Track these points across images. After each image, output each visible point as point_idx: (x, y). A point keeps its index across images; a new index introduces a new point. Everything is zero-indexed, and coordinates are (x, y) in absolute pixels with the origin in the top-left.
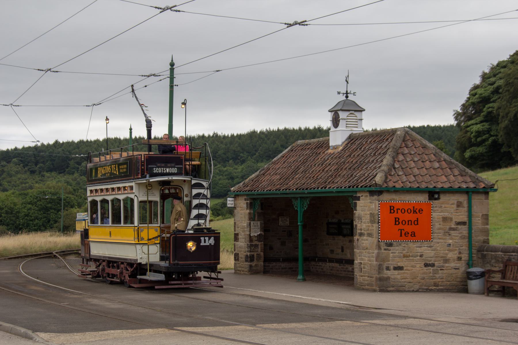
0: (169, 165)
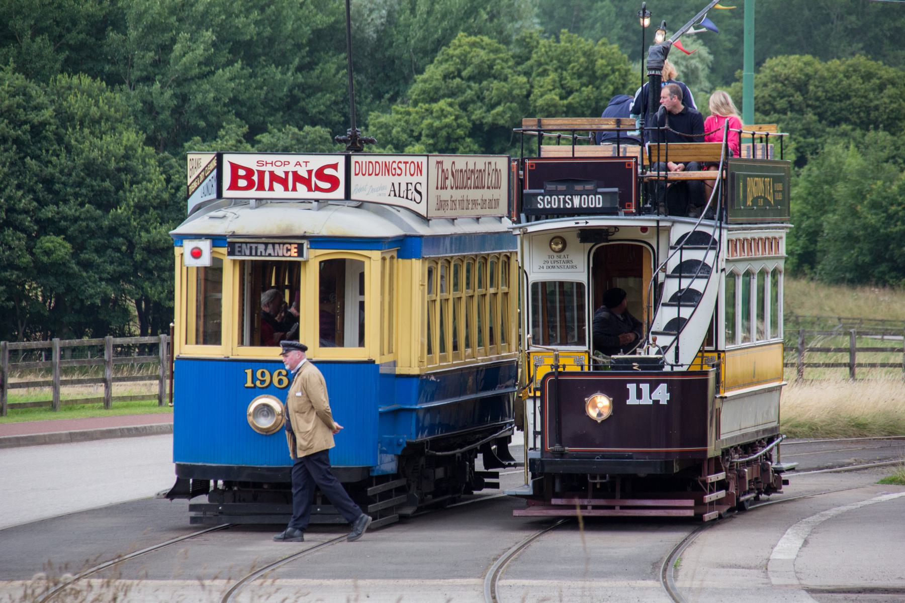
0: (578, 187)
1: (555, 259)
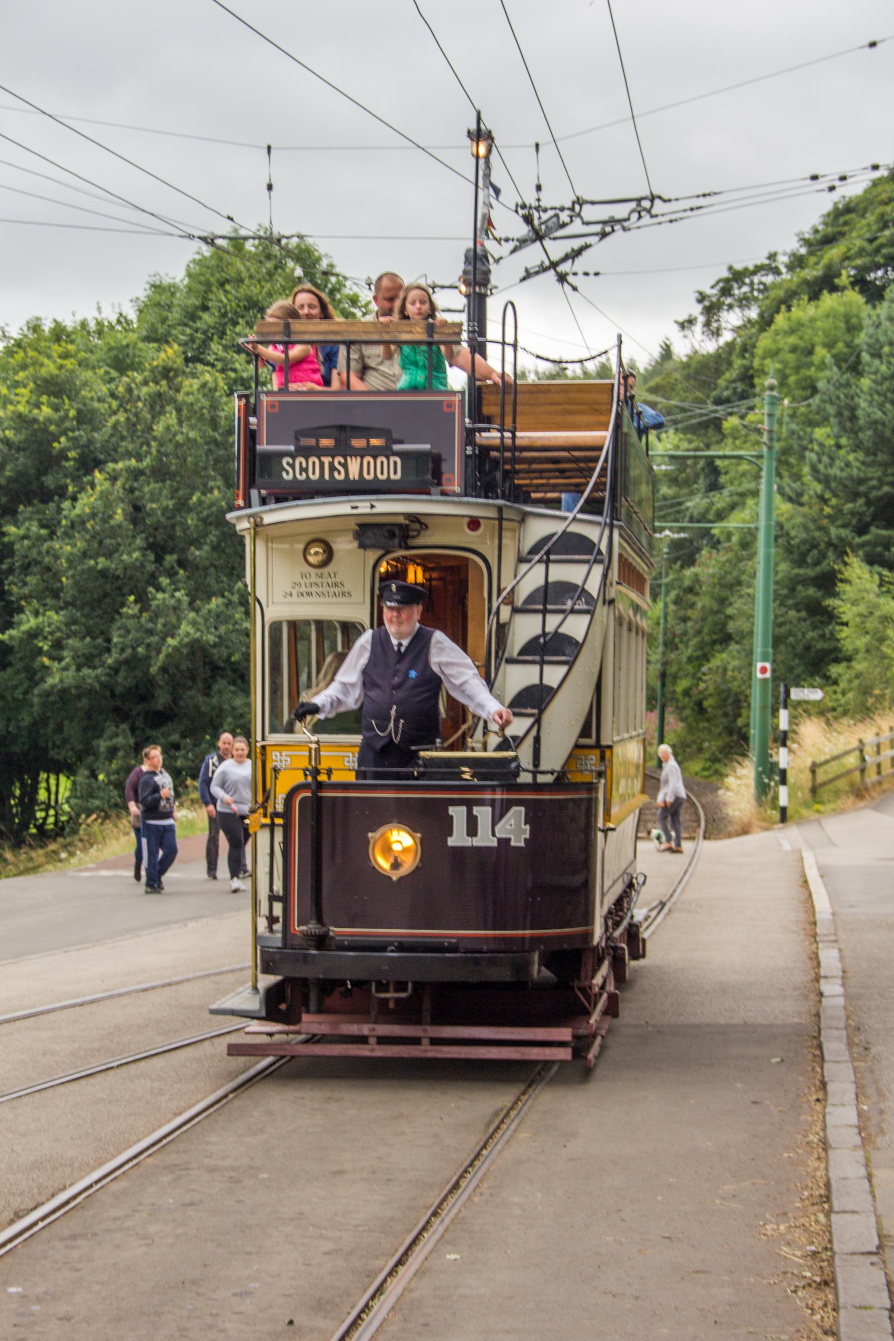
1: (314, 579)
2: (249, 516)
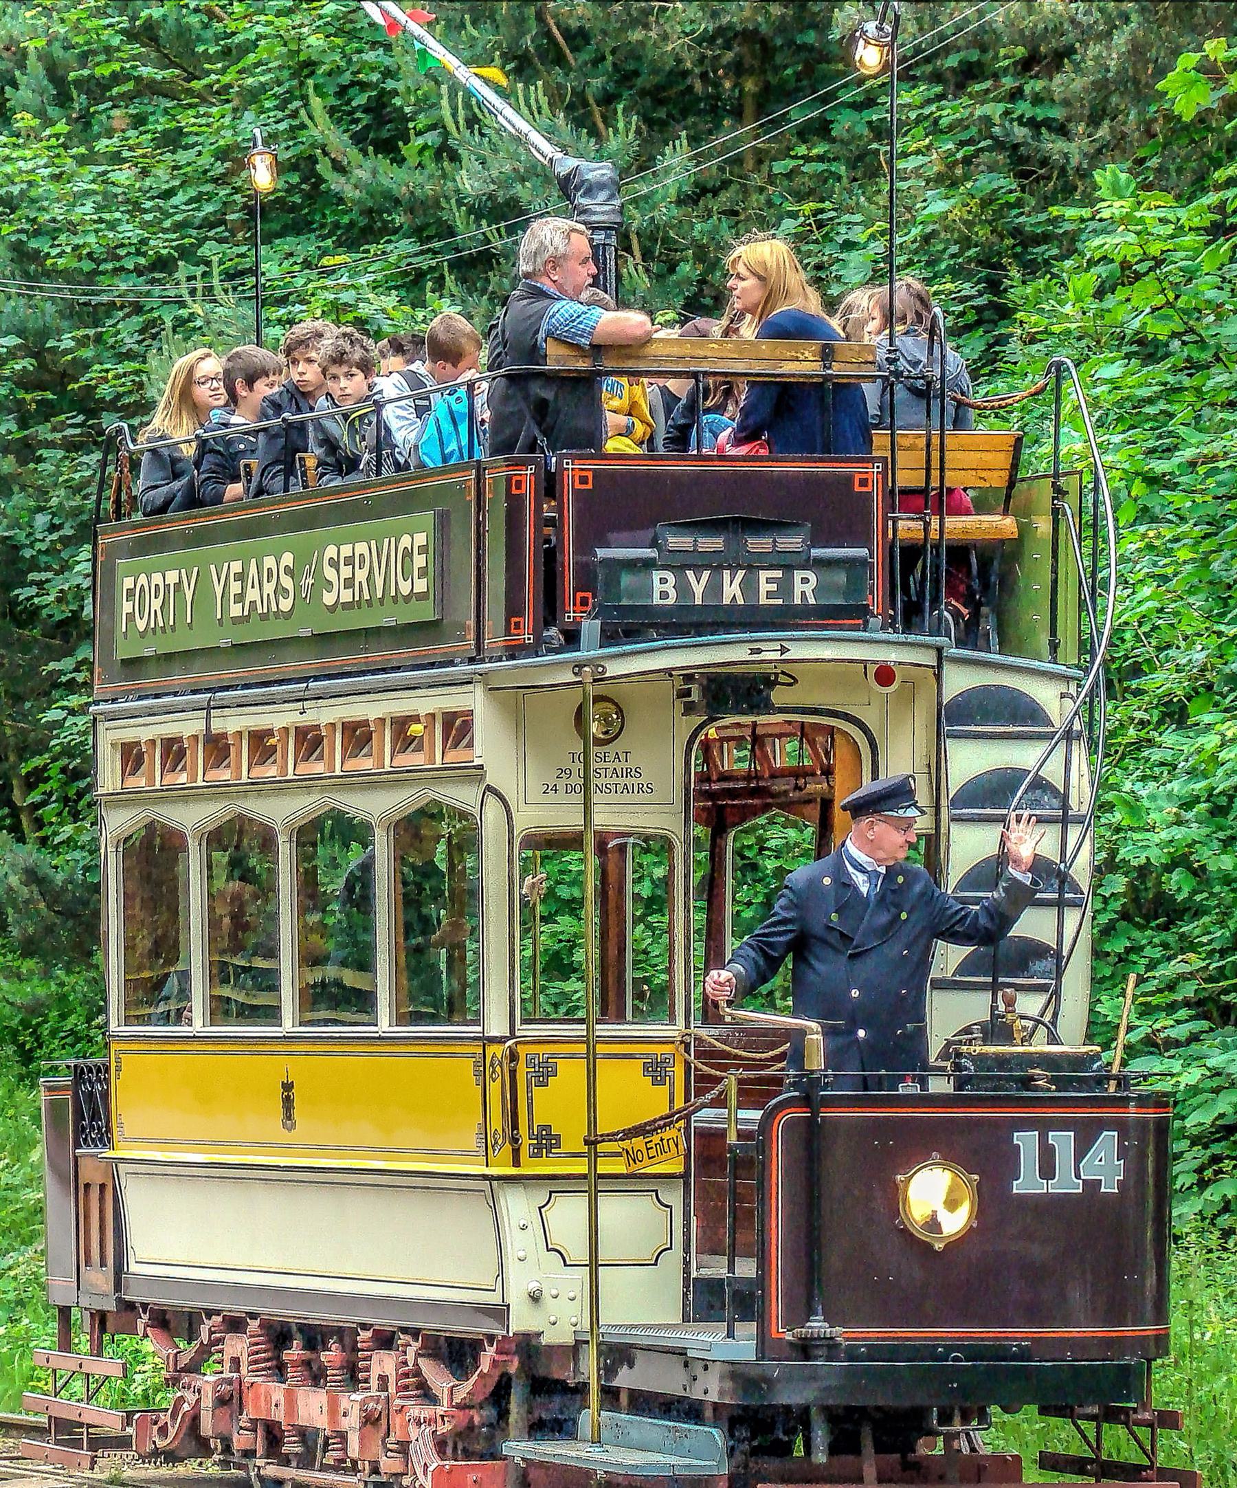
0: (758, 544)
2: (579, 666)
